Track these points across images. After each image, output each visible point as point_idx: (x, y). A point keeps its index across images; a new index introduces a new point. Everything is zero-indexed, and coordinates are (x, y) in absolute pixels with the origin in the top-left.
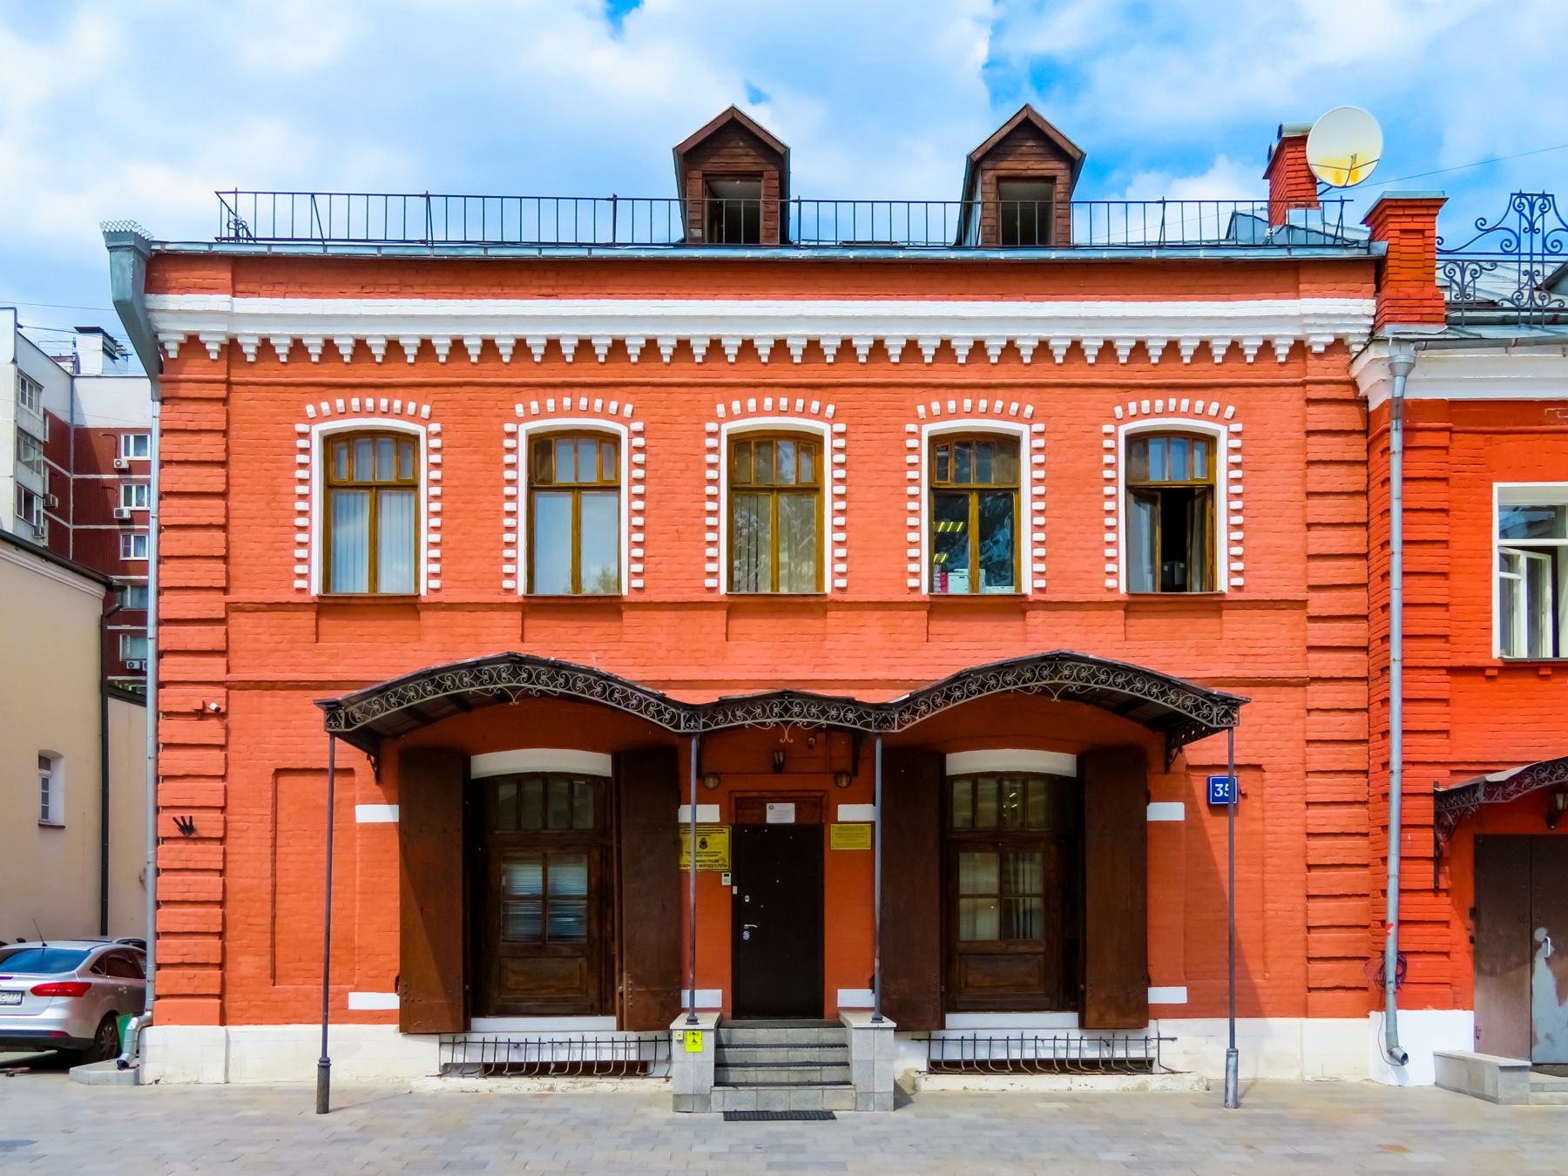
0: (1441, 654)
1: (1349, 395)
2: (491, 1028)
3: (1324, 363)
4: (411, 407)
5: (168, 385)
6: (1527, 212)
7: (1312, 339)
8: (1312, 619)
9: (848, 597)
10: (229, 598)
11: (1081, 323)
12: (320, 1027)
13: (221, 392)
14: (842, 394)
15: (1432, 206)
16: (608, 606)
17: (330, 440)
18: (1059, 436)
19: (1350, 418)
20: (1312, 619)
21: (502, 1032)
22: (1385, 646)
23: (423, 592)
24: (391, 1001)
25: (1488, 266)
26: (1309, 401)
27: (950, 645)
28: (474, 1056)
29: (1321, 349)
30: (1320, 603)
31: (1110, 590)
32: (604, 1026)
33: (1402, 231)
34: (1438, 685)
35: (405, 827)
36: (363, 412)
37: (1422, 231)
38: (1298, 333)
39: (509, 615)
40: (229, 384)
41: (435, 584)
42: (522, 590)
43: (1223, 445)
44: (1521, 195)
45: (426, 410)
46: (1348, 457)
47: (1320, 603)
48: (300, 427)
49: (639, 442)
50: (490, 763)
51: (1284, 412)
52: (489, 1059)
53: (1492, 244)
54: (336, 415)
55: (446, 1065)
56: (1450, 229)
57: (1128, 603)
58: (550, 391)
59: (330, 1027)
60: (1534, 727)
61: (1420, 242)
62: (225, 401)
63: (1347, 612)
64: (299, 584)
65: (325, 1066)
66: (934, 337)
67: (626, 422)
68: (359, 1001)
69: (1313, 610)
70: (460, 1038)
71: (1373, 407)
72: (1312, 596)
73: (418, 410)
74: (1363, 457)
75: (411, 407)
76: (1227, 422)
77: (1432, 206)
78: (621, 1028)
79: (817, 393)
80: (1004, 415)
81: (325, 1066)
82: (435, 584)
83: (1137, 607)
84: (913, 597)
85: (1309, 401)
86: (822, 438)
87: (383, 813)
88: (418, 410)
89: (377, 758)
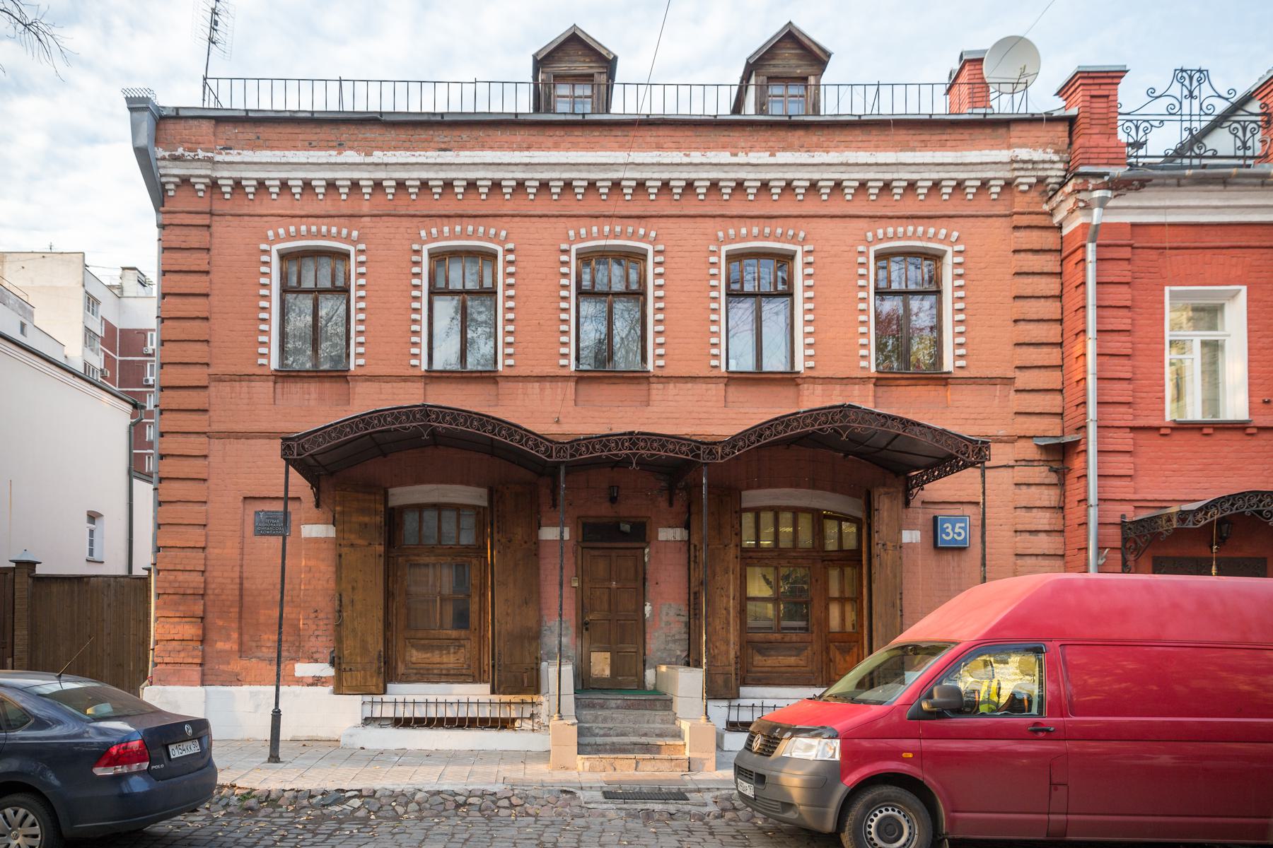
0: (1126, 417)
1: (1046, 223)
2: (398, 691)
3: (1027, 198)
4: (344, 232)
5: (168, 216)
6: (1187, 82)
7: (1019, 180)
8: (1017, 391)
9: (665, 373)
10: (211, 371)
11: (843, 168)
12: (274, 688)
13: (204, 220)
14: (663, 223)
15: (1114, 76)
16: (489, 377)
17: (285, 256)
18: (822, 254)
19: (1049, 240)
20: (1017, 391)
21: (410, 696)
22: (1081, 409)
23: (352, 367)
24: (327, 671)
25: (1156, 124)
26: (1016, 228)
27: (742, 410)
28: (389, 712)
29: (1025, 188)
30: (1024, 379)
31: (863, 368)
32: (480, 691)
33: (1092, 97)
34: (1123, 440)
35: (338, 542)
36: (310, 235)
37: (1107, 96)
38: (1009, 175)
39: (416, 385)
40: (211, 214)
41: (361, 361)
42: (424, 367)
43: (949, 260)
44: (1182, 70)
45: (355, 234)
46: (1046, 270)
47: (1024, 379)
48: (264, 247)
49: (511, 257)
50: (403, 495)
51: (995, 238)
52: (399, 714)
53: (1160, 106)
54: (289, 237)
55: (366, 719)
56: (1129, 96)
57: (878, 379)
58: (445, 220)
59: (282, 689)
60: (1200, 473)
61: (1104, 105)
62: (209, 226)
63: (1046, 387)
64: (261, 361)
65: (276, 715)
66: (731, 180)
67: (501, 243)
68: (304, 669)
69: (1019, 384)
70: (377, 698)
71: (1065, 232)
72: (1018, 374)
73: (349, 234)
74: (1058, 270)
75: (344, 232)
76: (952, 244)
77: (1114, 76)
78: (493, 692)
79: (643, 221)
80: (782, 238)
81: (276, 715)
82: (361, 361)
83: (884, 382)
84: (715, 373)
85: (1016, 228)
86: (645, 256)
87: (317, 530)
88: (349, 234)
89: (318, 489)
